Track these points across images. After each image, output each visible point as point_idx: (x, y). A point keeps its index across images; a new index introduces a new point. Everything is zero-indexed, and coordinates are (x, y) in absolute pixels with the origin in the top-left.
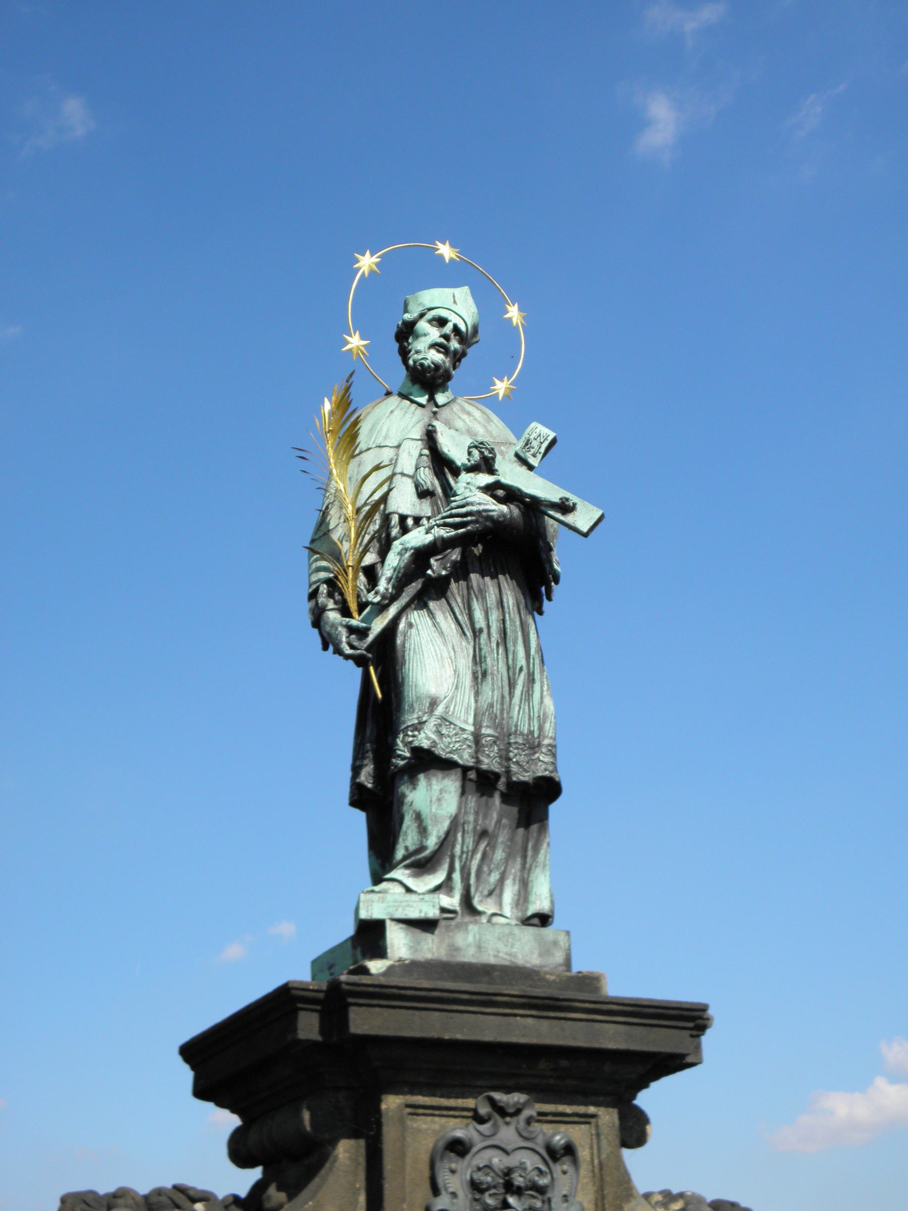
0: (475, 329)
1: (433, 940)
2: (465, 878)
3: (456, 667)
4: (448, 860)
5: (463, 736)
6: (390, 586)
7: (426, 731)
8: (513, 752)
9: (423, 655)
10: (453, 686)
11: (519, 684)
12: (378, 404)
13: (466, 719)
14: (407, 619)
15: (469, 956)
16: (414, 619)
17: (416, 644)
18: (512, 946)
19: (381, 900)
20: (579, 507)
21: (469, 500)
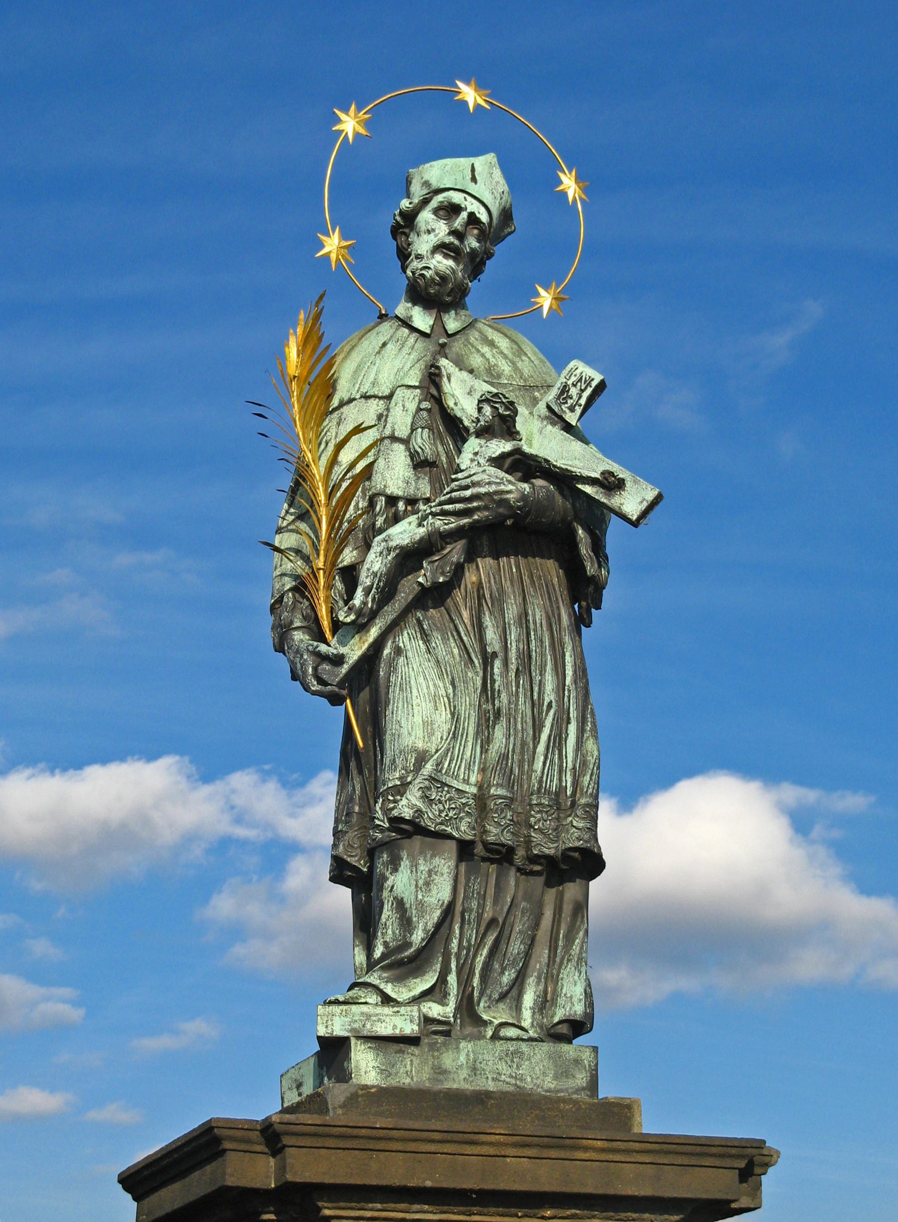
0: (507, 215)
1: (411, 1061)
2: (465, 981)
3: (455, 707)
4: (440, 959)
5: (460, 800)
6: (370, 599)
7: (409, 797)
8: (535, 817)
9: (411, 692)
10: (449, 734)
11: (547, 727)
12: (366, 333)
13: (466, 778)
14: (393, 642)
15: (460, 1081)
16: (403, 642)
17: (404, 678)
18: (518, 1068)
19: (344, 1013)
20: (628, 484)
21: (475, 478)
